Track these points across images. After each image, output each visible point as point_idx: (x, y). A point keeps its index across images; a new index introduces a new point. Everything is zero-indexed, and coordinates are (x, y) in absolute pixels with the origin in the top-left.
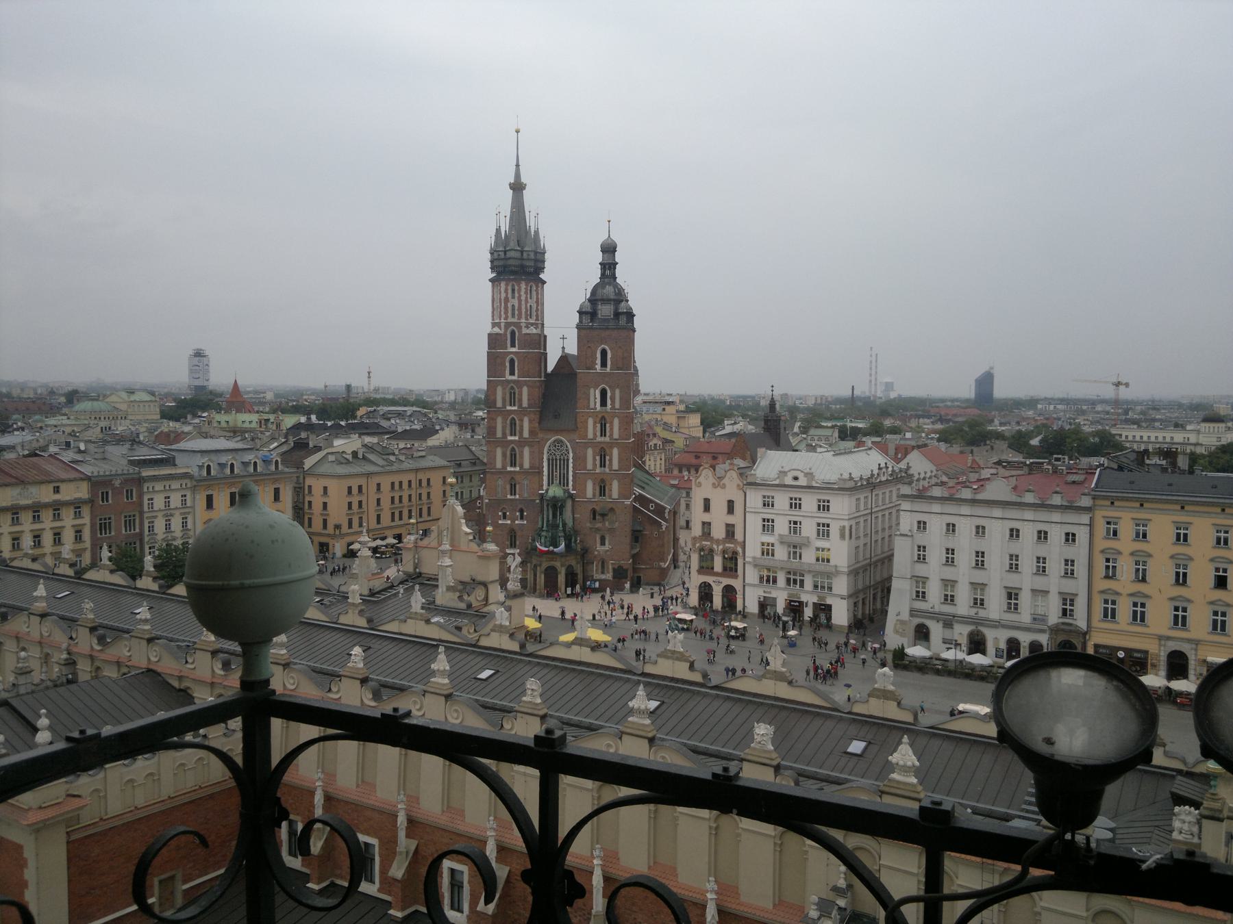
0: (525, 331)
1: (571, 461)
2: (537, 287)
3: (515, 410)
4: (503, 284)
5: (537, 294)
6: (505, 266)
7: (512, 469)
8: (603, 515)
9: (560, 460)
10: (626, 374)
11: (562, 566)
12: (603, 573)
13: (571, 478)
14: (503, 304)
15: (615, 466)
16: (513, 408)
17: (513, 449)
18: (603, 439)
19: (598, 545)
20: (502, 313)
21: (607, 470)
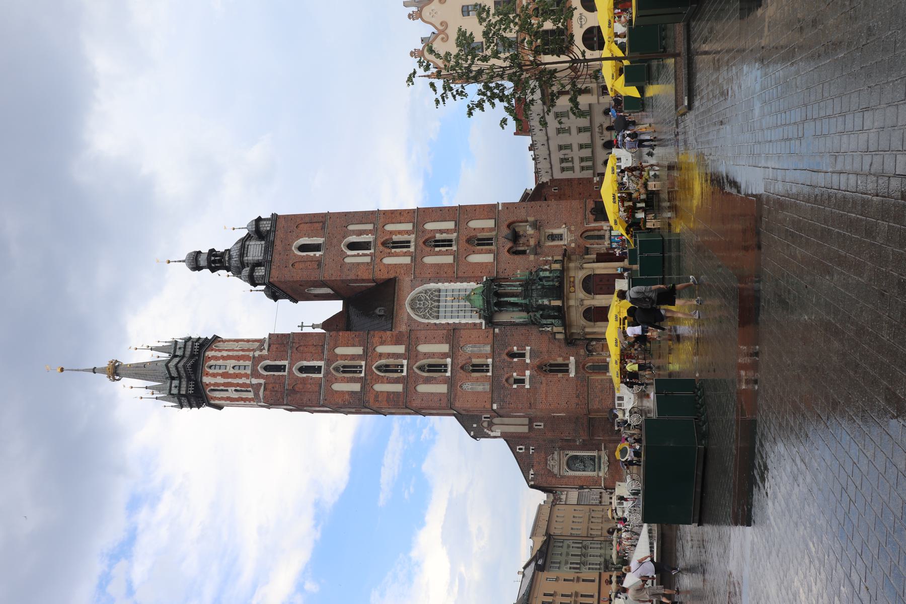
0: (265, 352)
3: (366, 365)
4: (206, 380)
6: (189, 379)
7: (449, 369)
8: (515, 237)
11: (582, 268)
14: (229, 380)
16: (364, 368)
17: (421, 368)
18: (412, 244)
19: (561, 243)
20: (240, 381)
21: (455, 234)
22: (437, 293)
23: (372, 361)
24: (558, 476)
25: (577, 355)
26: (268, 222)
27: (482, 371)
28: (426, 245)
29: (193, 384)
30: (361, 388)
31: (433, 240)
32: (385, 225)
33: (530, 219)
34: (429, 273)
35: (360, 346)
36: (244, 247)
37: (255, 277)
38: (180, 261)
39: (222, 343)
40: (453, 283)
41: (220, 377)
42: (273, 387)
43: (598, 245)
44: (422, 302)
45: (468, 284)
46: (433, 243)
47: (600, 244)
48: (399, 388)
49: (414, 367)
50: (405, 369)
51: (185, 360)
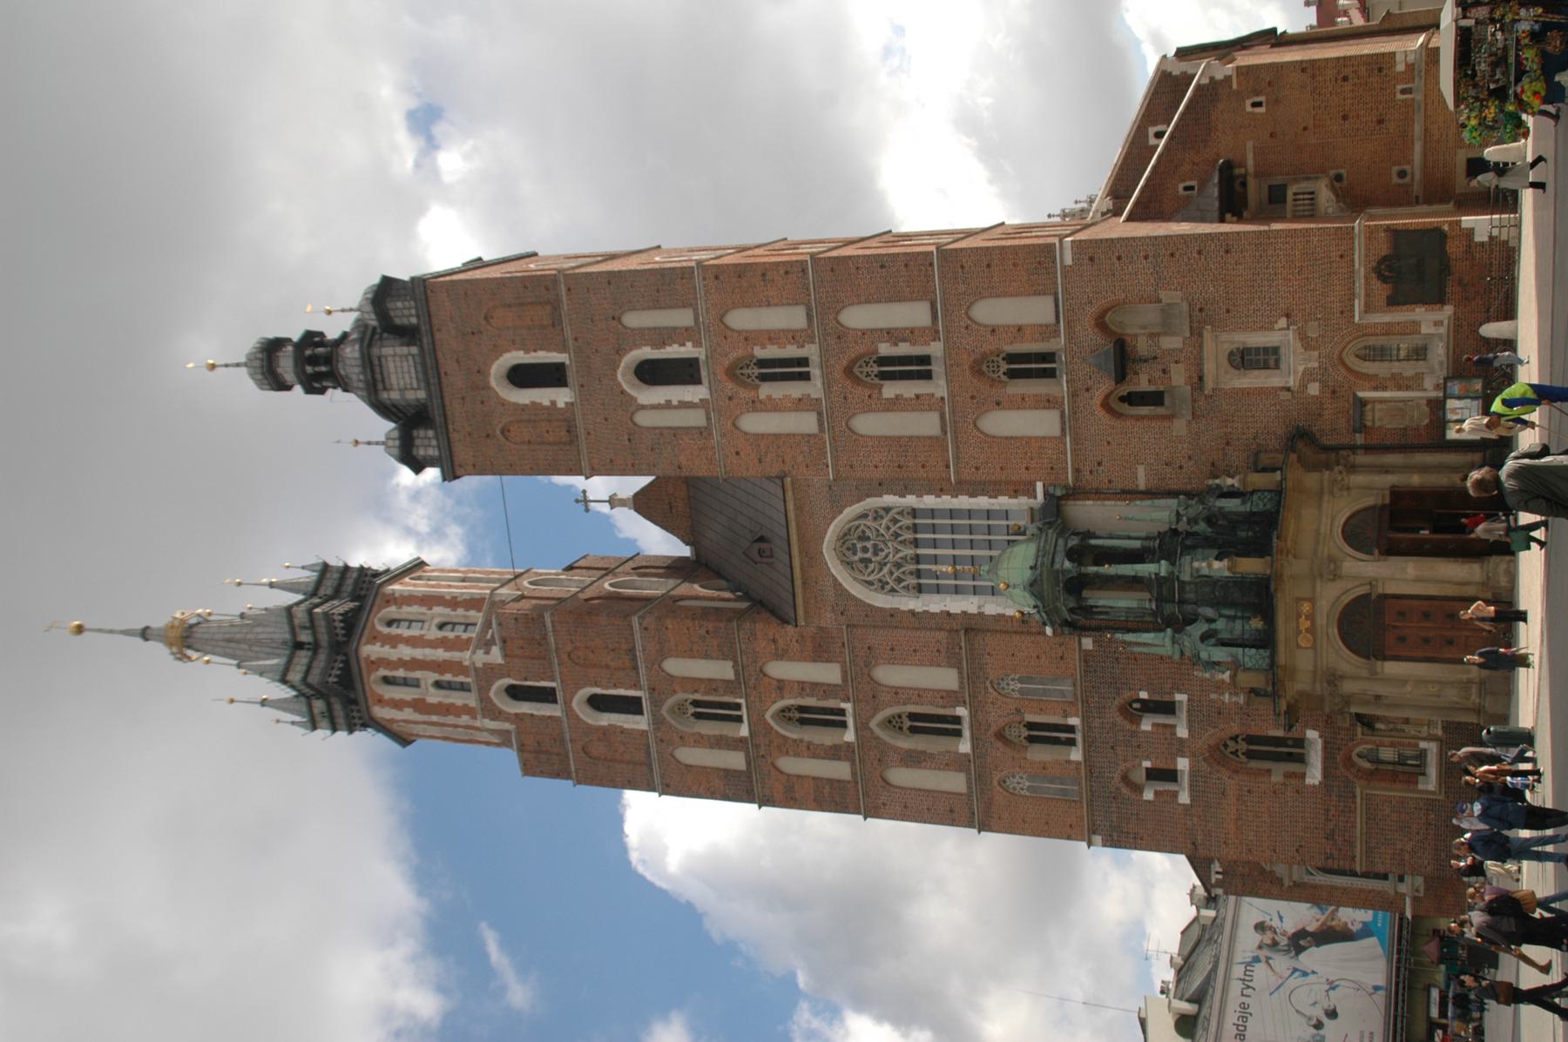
0: (496, 655)
1: (911, 500)
2: (392, 600)
5: (410, 599)
7: (967, 733)
8: (1123, 359)
9: (916, 543)
10: (569, 290)
12: (1420, 353)
13: (983, 502)
14: (434, 718)
15: (914, 314)
16: (744, 712)
17: (892, 723)
18: (815, 371)
19: (1273, 380)
22: (908, 521)
23: (761, 701)
24: (1287, 883)
25: (1328, 725)
26: (407, 303)
27: (1056, 741)
28: (857, 380)
29: (359, 711)
30: (748, 763)
31: (874, 358)
32: (726, 312)
33: (1163, 295)
34: (876, 467)
35: (724, 659)
36: (371, 363)
37: (420, 458)
38: (238, 365)
39: (393, 608)
40: (949, 497)
41: (411, 710)
42: (538, 743)
43: (1399, 388)
44: (869, 544)
45: (993, 501)
46: (876, 369)
47: (1408, 388)
48: (840, 770)
49: (873, 724)
50: (850, 721)
51: (322, 656)
